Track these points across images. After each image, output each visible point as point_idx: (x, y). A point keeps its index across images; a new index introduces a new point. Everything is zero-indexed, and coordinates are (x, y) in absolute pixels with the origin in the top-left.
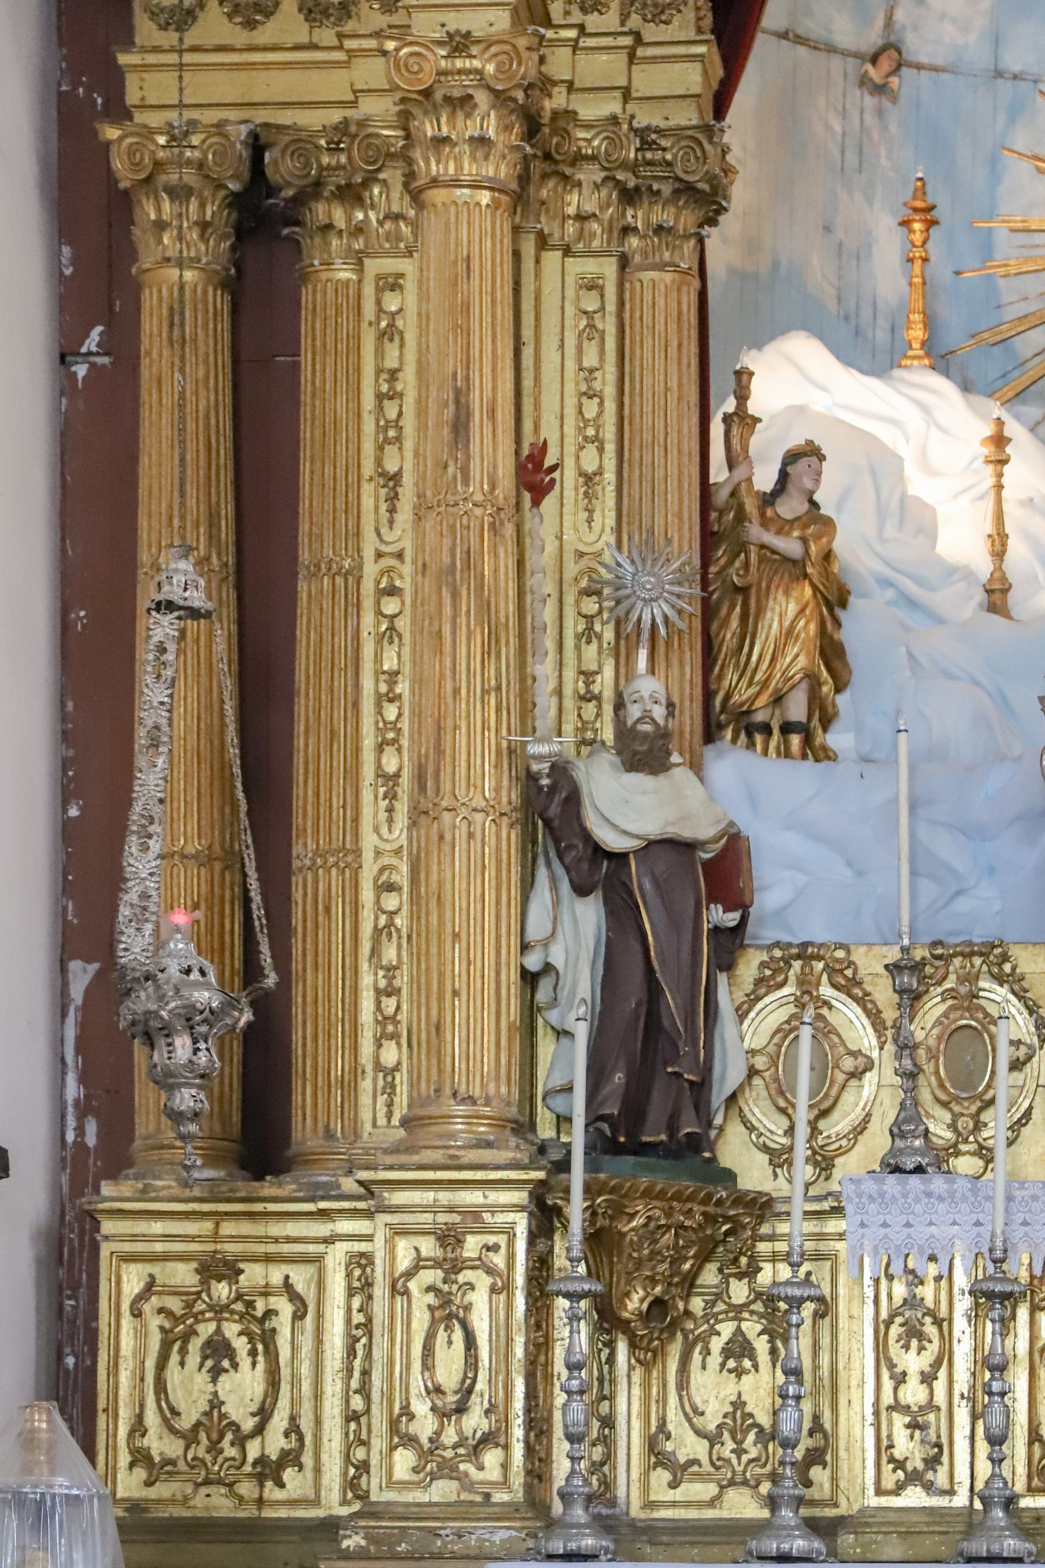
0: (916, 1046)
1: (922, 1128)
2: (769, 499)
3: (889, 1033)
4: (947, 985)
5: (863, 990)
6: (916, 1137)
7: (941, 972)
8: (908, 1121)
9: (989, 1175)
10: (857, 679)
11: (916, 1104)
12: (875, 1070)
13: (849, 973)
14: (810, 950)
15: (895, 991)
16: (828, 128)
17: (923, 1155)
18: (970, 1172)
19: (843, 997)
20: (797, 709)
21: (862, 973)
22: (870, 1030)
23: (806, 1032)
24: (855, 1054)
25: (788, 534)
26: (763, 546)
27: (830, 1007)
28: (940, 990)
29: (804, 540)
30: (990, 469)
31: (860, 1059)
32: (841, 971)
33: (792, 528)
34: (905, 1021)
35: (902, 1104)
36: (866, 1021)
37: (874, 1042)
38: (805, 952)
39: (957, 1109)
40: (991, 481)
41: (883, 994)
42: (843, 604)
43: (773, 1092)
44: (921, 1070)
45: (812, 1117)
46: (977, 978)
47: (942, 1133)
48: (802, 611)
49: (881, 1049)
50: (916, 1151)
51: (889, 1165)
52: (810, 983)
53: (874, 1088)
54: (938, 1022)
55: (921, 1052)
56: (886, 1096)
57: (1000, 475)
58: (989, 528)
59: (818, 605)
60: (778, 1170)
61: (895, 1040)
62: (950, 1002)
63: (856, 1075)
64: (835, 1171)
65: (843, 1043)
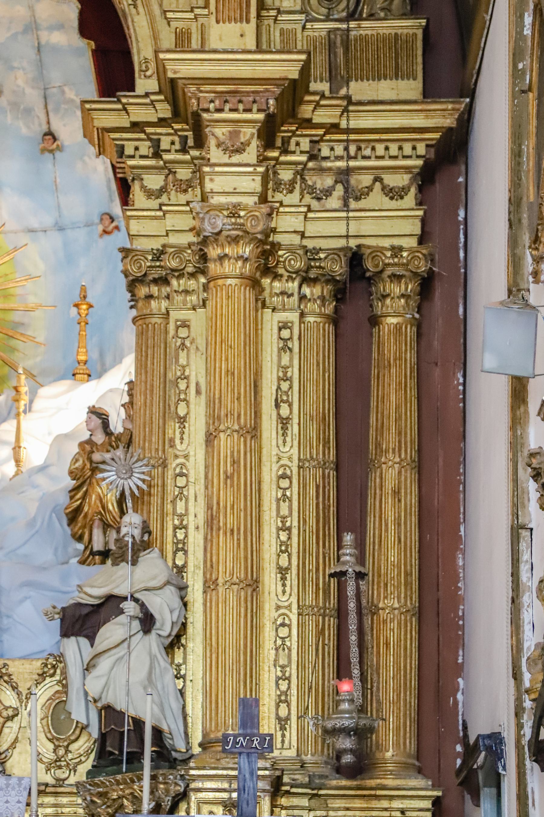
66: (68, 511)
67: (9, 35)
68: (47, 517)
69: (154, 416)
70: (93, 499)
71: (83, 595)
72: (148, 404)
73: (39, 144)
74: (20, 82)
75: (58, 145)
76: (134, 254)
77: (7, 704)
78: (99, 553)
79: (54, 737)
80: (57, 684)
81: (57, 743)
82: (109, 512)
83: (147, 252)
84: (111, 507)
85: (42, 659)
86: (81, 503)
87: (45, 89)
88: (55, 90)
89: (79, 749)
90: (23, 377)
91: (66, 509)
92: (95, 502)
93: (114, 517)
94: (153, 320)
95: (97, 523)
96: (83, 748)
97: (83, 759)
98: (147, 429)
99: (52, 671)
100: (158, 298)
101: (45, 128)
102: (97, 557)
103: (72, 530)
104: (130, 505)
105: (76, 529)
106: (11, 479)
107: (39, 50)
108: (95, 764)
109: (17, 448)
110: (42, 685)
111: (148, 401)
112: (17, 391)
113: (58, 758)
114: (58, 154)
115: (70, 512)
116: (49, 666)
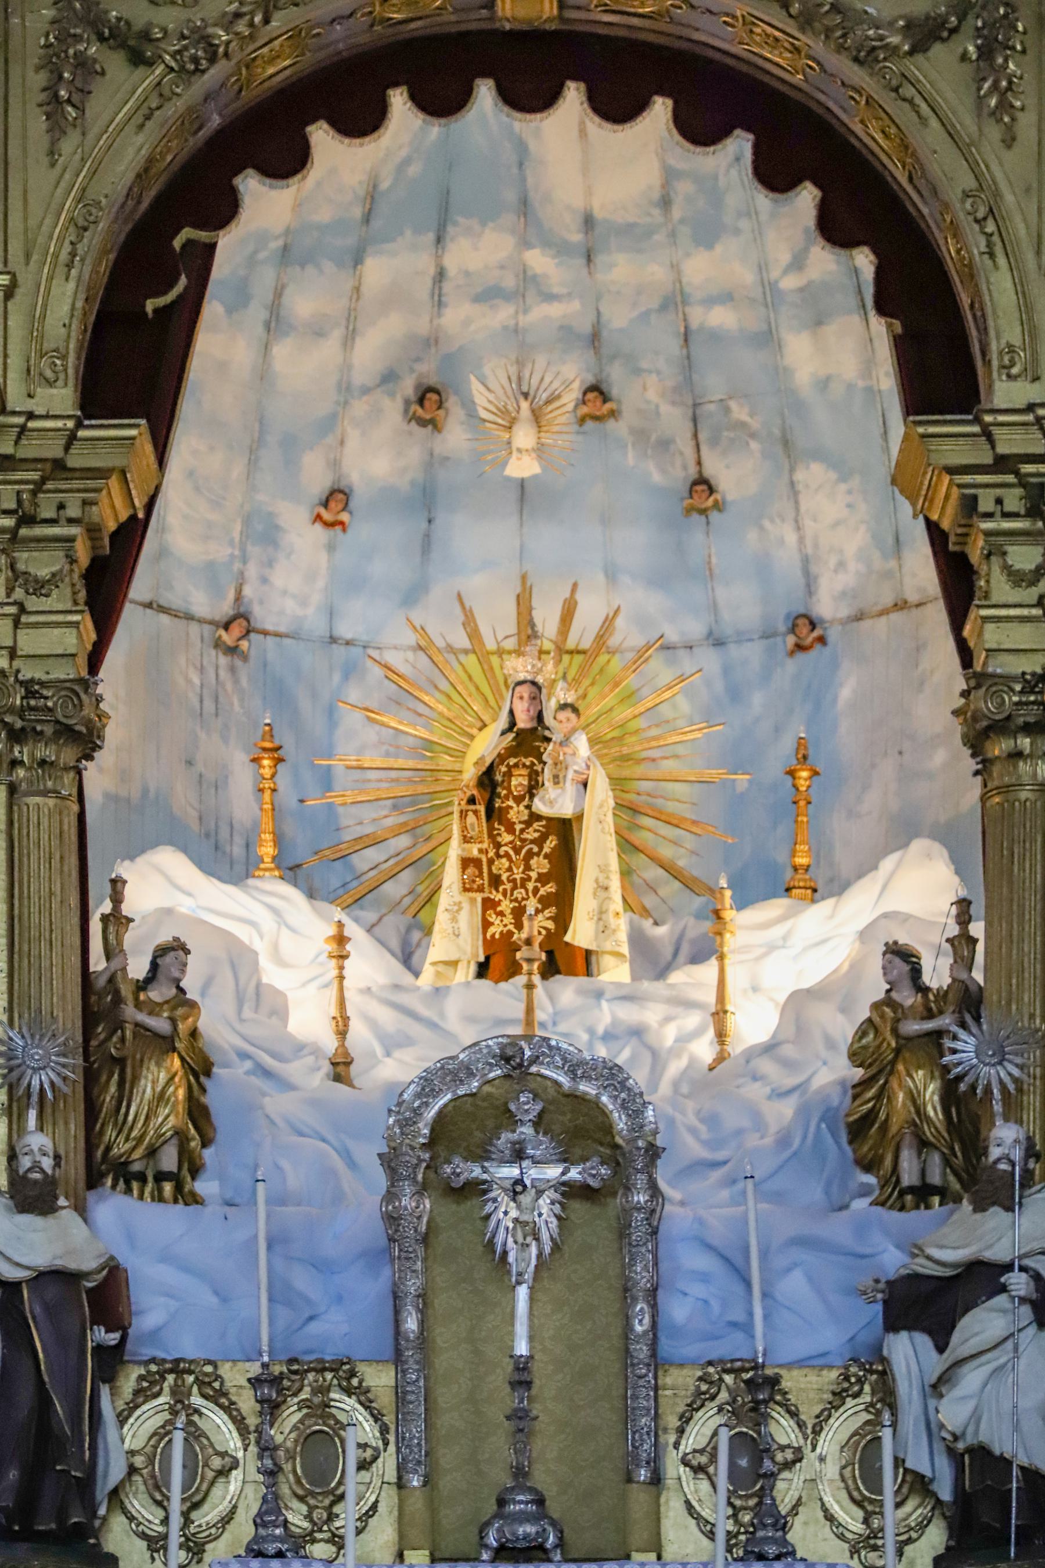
0: (276, 1448)
1: (282, 1518)
2: (143, 985)
3: (252, 1437)
4: (303, 1396)
5: (229, 1400)
6: (277, 1527)
7: (297, 1385)
8: (268, 1512)
9: (341, 1559)
10: (220, 1137)
11: (277, 1497)
12: (240, 1469)
13: (217, 1385)
14: (182, 1365)
15: (257, 1401)
16: (189, 681)
17: (282, 1542)
18: (324, 1557)
19: (211, 1405)
20: (169, 1161)
21: (228, 1384)
22: (235, 1434)
23: (178, 1437)
24: (223, 1455)
25: (158, 1015)
26: (137, 1025)
27: (201, 1414)
28: (296, 1400)
29: (173, 1021)
30: (333, 962)
31: (227, 1459)
32: (210, 1384)
33: (162, 1010)
34: (267, 1427)
35: (264, 1499)
36: (231, 1426)
37: (239, 1444)
38: (178, 1368)
39: (312, 1502)
40: (335, 972)
41: (247, 1403)
42: (208, 1074)
43: (150, 1487)
44: (281, 1469)
45: (185, 1508)
46: (328, 1390)
47: (299, 1523)
48: (172, 1078)
49: (245, 1450)
50: (277, 1539)
51: (253, 1550)
52: (182, 1393)
53: (239, 1484)
54: (295, 1428)
55: (281, 1453)
56: (249, 1490)
57: (341, 968)
58: (333, 1011)
59: (186, 1074)
60: (155, 1555)
61: (258, 1442)
62: (305, 1411)
63: (223, 1473)
64: (205, 1555)
65: (212, 1445)
66: (851, 1119)
67: (635, 314)
68: (812, 1129)
69: (1026, 960)
70: (900, 1099)
71: (921, 1260)
72: (1015, 939)
73: (682, 499)
74: (652, 395)
75: (716, 502)
76: (990, 682)
77: (783, 1440)
78: (911, 1190)
79: (865, 1498)
80: (866, 1410)
81: (870, 1508)
82: (928, 1119)
83: (1013, 678)
84: (932, 1113)
85: (838, 1368)
86: (874, 1106)
87: (695, 405)
88: (712, 407)
89: (905, 1519)
90: (728, 893)
91: (847, 1115)
92: (904, 1104)
93: (936, 1128)
94: (1023, 795)
95: (908, 1139)
96: (914, 1517)
97: (914, 1535)
98: (1014, 981)
99: (856, 1388)
100: (1030, 756)
101: (692, 472)
102: (909, 1198)
103: (855, 1151)
104: (998, 1107)
105: (865, 1149)
106: (711, 1069)
107: (686, 340)
108: (952, 1543)
109: (720, 1014)
110: (841, 1410)
111: (1015, 933)
112: (719, 918)
113: (872, 1532)
114: (714, 516)
115: (856, 1121)
116: (853, 1380)
